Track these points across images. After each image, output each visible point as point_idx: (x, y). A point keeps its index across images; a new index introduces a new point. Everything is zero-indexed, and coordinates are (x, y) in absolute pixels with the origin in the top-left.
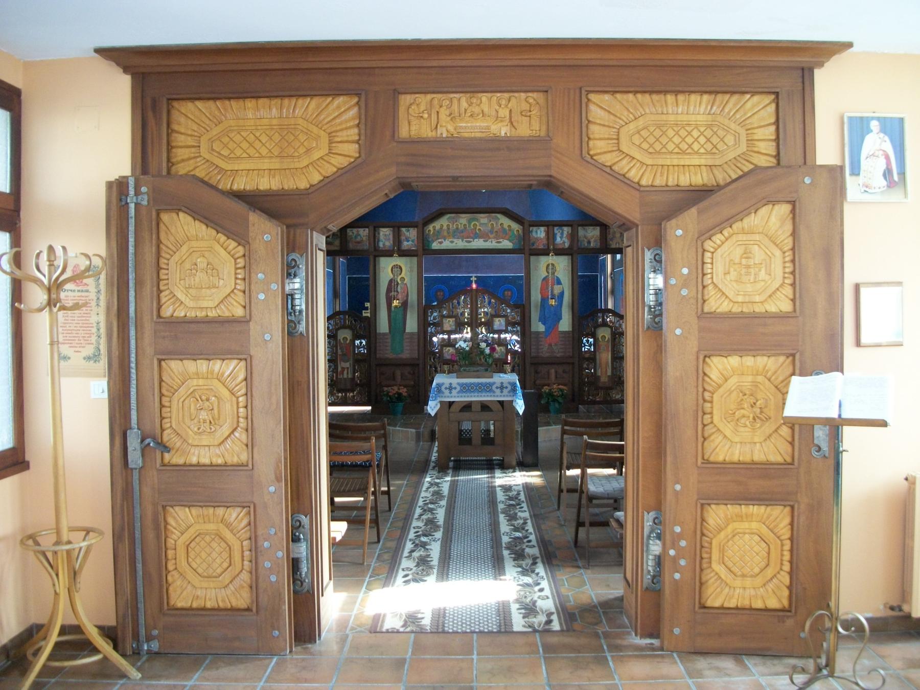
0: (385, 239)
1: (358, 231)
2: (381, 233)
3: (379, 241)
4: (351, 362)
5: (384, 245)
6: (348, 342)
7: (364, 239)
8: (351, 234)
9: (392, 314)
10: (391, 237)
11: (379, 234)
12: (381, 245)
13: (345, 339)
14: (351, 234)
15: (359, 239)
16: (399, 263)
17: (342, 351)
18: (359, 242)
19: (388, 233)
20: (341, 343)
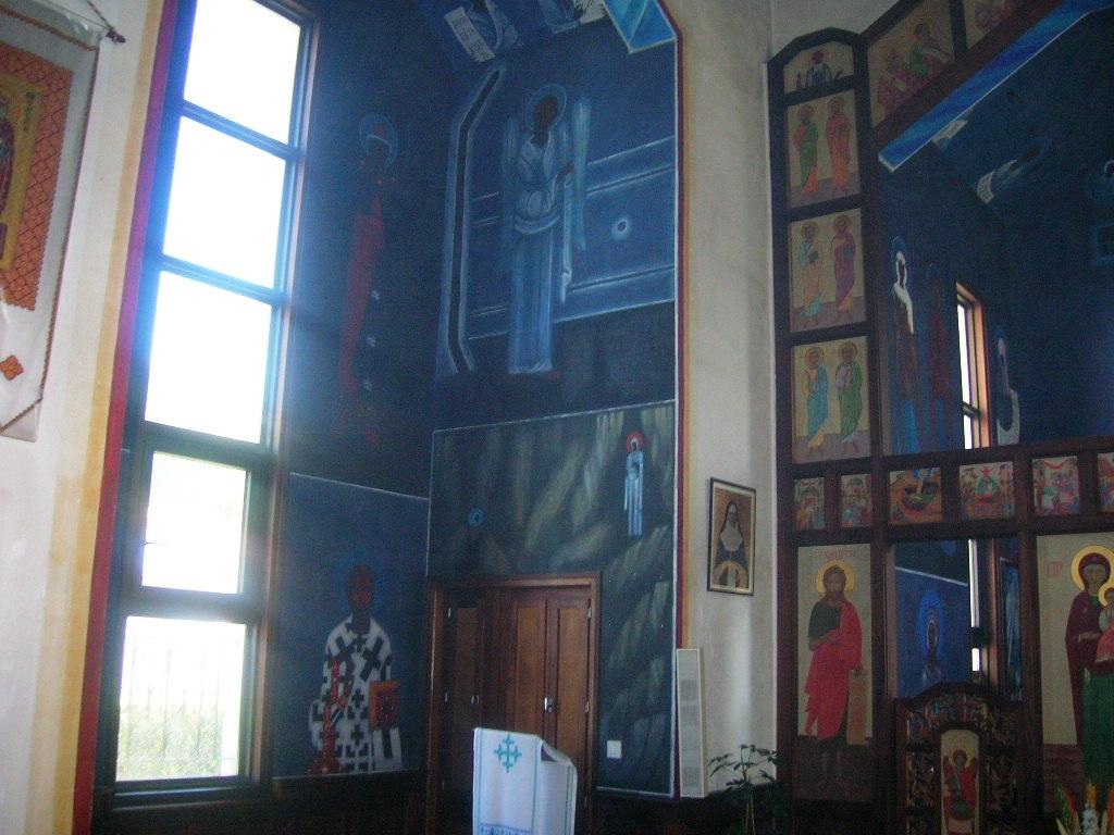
0: (1060, 488)
1: (986, 471)
2: (1048, 473)
3: (1041, 494)
4: (976, 821)
5: (1056, 502)
6: (967, 765)
7: (1004, 489)
8: (968, 479)
9: (1087, 693)
10: (1075, 482)
11: (1042, 473)
12: (1048, 502)
13: (960, 755)
14: (968, 479)
15: (990, 490)
16: (1099, 550)
17: (953, 791)
18: (987, 500)
19: (1064, 470)
20: (949, 770)
